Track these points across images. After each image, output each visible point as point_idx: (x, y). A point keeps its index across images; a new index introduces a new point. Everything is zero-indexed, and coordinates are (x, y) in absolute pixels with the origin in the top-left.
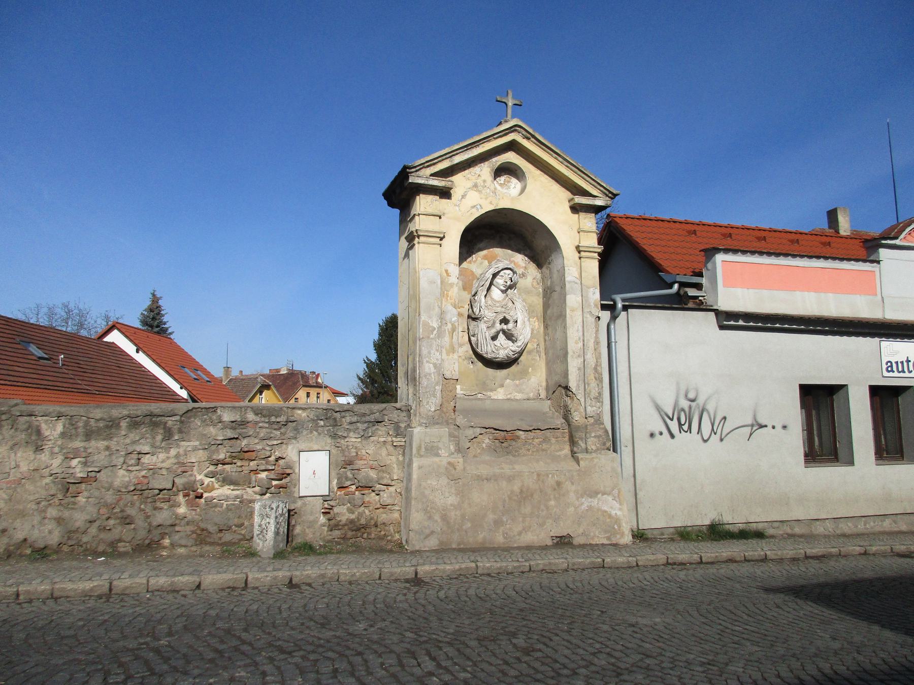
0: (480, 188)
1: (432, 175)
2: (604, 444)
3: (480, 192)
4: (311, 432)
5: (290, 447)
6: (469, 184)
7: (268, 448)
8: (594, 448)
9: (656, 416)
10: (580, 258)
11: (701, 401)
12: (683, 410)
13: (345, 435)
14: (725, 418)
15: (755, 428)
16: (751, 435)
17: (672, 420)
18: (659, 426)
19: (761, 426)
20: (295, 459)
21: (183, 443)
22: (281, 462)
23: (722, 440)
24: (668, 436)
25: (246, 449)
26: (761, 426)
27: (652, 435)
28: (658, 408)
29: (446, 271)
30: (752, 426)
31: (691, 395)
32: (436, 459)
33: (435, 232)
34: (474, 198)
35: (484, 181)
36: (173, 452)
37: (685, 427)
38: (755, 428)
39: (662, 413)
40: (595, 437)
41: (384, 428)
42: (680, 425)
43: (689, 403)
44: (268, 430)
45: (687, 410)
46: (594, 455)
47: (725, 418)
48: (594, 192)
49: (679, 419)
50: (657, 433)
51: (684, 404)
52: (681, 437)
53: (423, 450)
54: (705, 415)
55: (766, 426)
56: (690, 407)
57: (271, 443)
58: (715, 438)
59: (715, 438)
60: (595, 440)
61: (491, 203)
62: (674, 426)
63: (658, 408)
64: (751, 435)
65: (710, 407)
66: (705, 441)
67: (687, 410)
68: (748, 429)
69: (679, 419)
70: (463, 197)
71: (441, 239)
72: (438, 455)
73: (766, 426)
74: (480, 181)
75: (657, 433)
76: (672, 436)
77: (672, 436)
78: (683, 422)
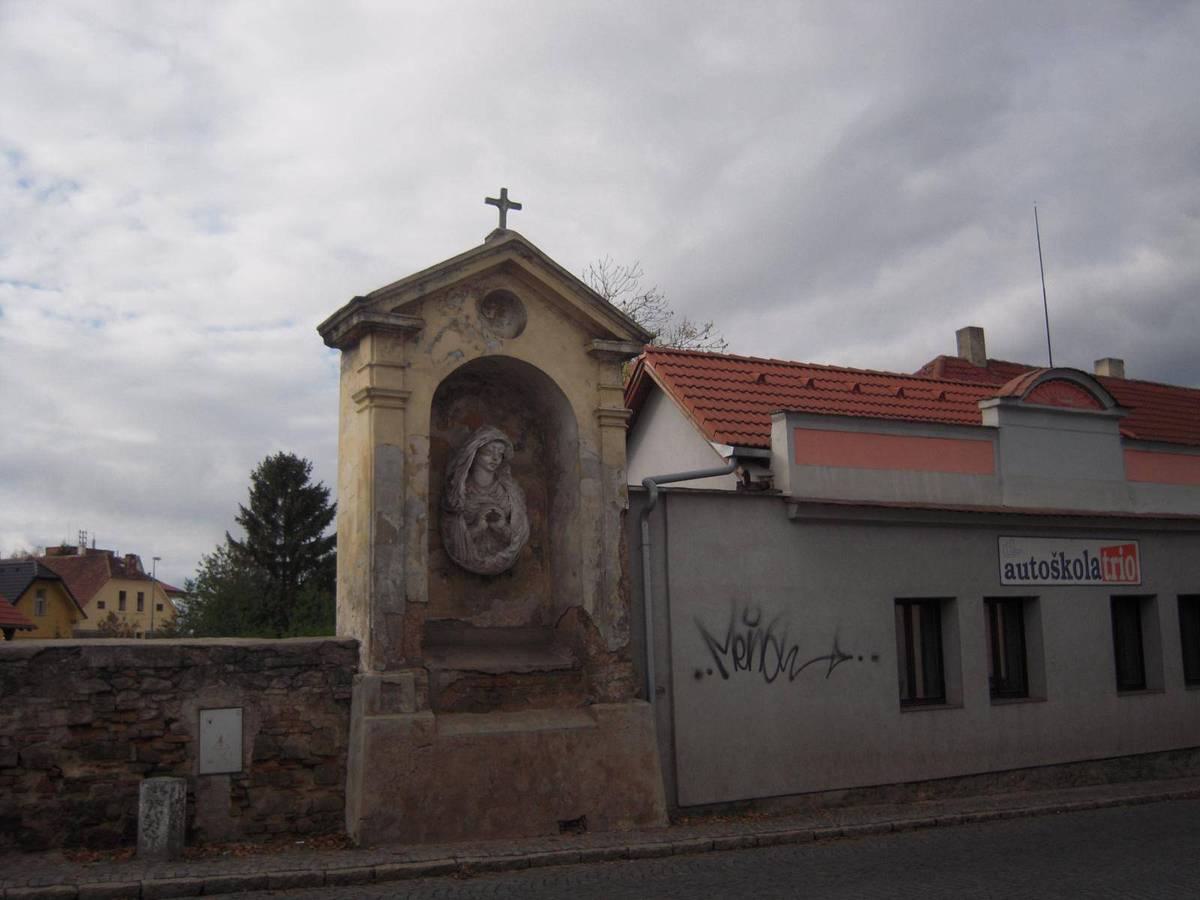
0: (462, 327)
1: (393, 310)
2: (632, 689)
3: (460, 332)
4: (216, 682)
5: (186, 704)
6: (445, 321)
7: (154, 706)
8: (617, 695)
9: (702, 644)
10: (601, 426)
11: (764, 625)
12: (740, 638)
13: (265, 684)
14: (796, 648)
15: (835, 662)
16: (830, 670)
17: (725, 652)
19: (845, 658)
20: (193, 719)
21: (31, 700)
22: (174, 726)
23: (792, 678)
24: (720, 675)
25: (122, 707)
26: (845, 658)
27: (698, 675)
28: (707, 637)
29: (412, 447)
30: (832, 657)
31: (752, 617)
32: (395, 717)
33: (392, 391)
34: (452, 340)
35: (467, 317)
36: (17, 714)
37: (743, 663)
38: (835, 662)
40: (619, 679)
41: (320, 674)
42: (736, 660)
43: (748, 628)
44: (154, 680)
45: (745, 637)
46: (619, 705)
47: (796, 648)
48: (622, 334)
49: (735, 652)
50: (704, 670)
51: (742, 629)
52: (738, 677)
53: (378, 704)
54: (770, 644)
55: (851, 657)
56: (750, 634)
57: (156, 698)
58: (783, 676)
59: (783, 676)
60: (618, 684)
61: (476, 348)
62: (728, 661)
63: (707, 637)
64: (830, 670)
65: (775, 633)
66: (769, 681)
67: (745, 637)
68: (825, 664)
69: (735, 652)
70: (438, 339)
71: (405, 400)
72: (398, 711)
73: (851, 657)
76: (725, 675)
77: (725, 675)
78: (740, 655)
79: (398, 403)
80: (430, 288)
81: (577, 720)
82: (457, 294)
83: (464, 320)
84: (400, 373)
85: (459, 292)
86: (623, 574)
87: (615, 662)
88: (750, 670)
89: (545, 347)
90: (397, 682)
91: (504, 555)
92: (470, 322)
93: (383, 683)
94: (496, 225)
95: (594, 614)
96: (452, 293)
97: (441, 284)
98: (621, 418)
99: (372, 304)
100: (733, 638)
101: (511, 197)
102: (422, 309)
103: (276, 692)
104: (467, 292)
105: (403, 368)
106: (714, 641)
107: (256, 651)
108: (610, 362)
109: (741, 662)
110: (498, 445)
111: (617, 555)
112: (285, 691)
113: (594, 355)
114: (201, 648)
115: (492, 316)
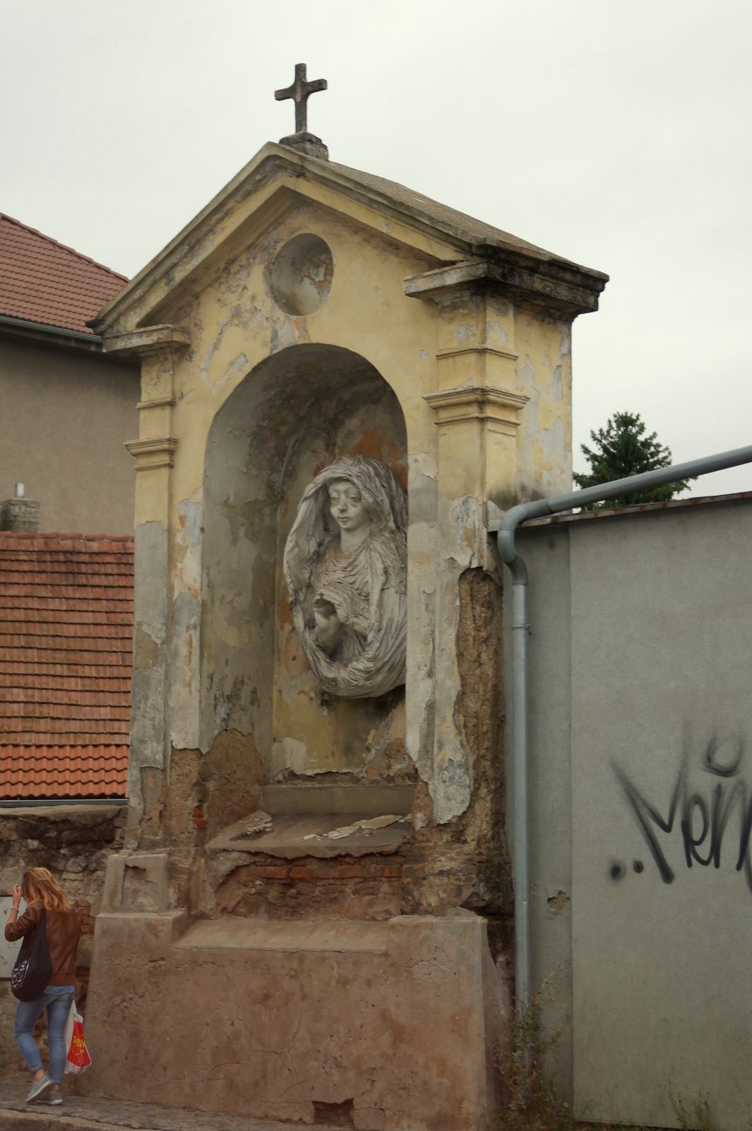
1: (140, 325)
9: (628, 820)
12: (698, 800)
17: (667, 828)
18: (634, 848)
24: (657, 873)
27: (616, 872)
28: (634, 798)
35: (253, 298)
37: (704, 850)
39: (644, 811)
42: (690, 844)
45: (709, 798)
49: (686, 828)
50: (629, 865)
51: (703, 783)
52: (692, 878)
56: (719, 792)
62: (672, 845)
63: (634, 798)
67: (709, 798)
69: (686, 828)
70: (216, 346)
71: (171, 452)
74: (246, 303)
75: (629, 865)
76: (667, 875)
77: (667, 875)
78: (696, 836)
79: (165, 459)
80: (180, 275)
81: (372, 941)
82: (241, 266)
83: (248, 303)
84: (167, 411)
85: (244, 262)
86: (463, 685)
87: (448, 842)
88: (717, 865)
89: (365, 313)
90: (141, 865)
91: (360, 666)
92: (258, 304)
93: (127, 867)
94: (290, 130)
95: (420, 758)
96: (234, 268)
97: (196, 262)
98: (469, 403)
99: (110, 326)
100: (685, 800)
101: (311, 77)
102: (199, 303)
103: (73, 876)
104: (254, 258)
105: (172, 404)
106: (645, 803)
107: (54, 823)
108: (454, 307)
109: (697, 848)
110: (342, 487)
111: (454, 652)
112: (80, 876)
113: (427, 297)
114: (15, 818)
115: (321, 277)
